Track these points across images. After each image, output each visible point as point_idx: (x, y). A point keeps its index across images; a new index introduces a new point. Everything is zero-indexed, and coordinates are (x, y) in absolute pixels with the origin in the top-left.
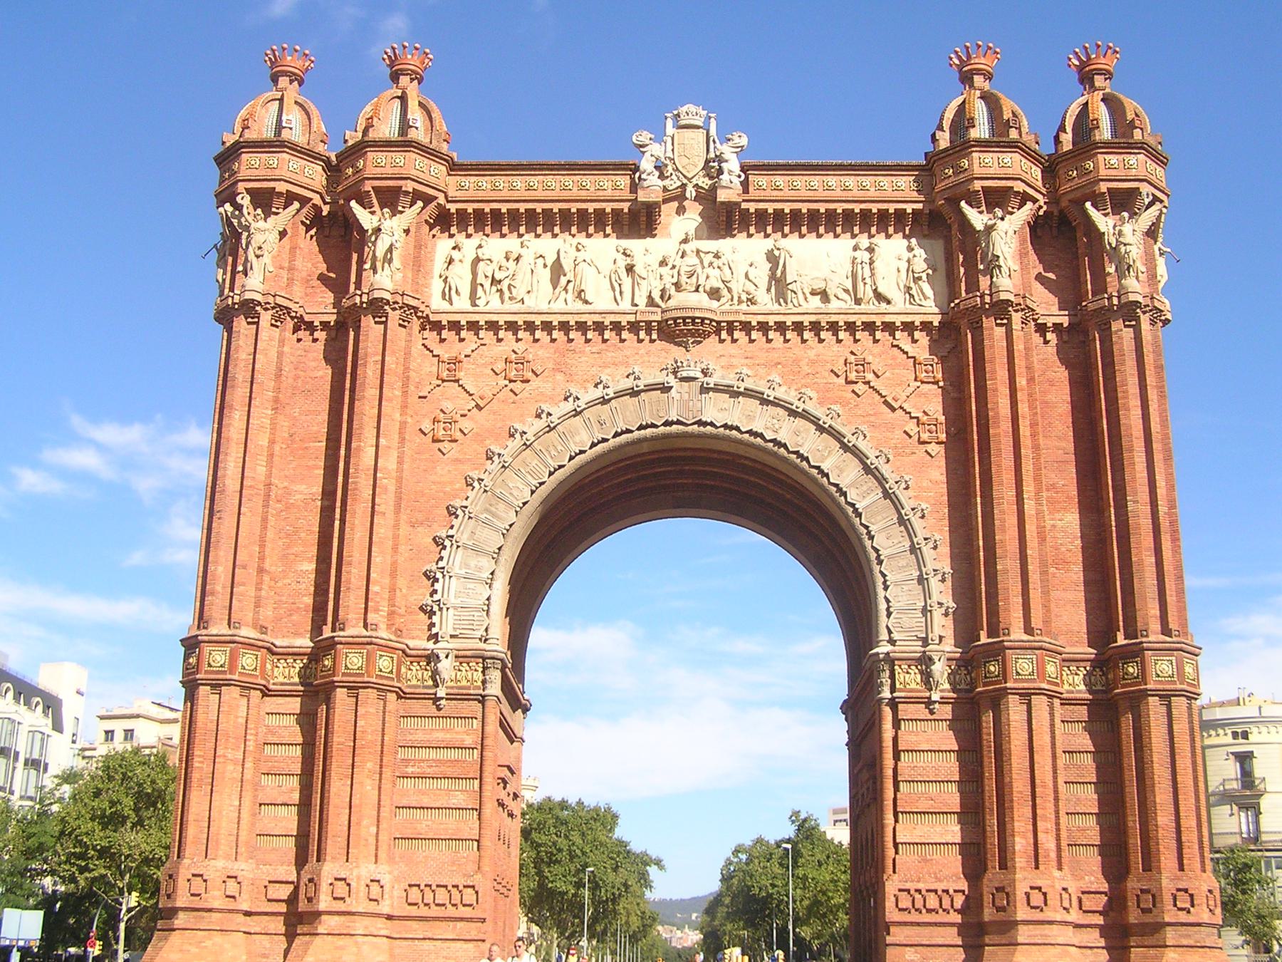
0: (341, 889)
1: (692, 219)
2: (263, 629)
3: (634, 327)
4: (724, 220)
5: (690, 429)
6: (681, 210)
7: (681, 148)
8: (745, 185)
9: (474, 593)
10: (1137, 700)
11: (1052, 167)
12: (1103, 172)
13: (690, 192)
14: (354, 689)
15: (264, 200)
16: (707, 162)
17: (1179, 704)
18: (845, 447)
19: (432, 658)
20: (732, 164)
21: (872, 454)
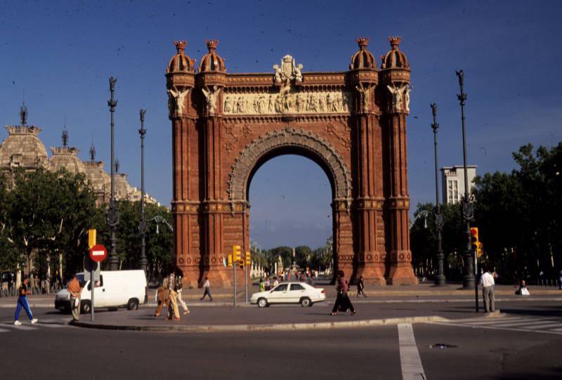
0: (214, 260)
1: (288, 88)
2: (190, 200)
3: (275, 119)
4: (296, 88)
5: (290, 145)
6: (285, 86)
7: (287, 68)
8: (303, 79)
9: (238, 187)
10: (394, 211)
11: (380, 74)
12: (392, 77)
13: (288, 81)
14: (213, 214)
15: (181, 89)
16: (292, 72)
17: (404, 212)
18: (327, 149)
19: (230, 204)
20: (299, 74)
21: (334, 151)
